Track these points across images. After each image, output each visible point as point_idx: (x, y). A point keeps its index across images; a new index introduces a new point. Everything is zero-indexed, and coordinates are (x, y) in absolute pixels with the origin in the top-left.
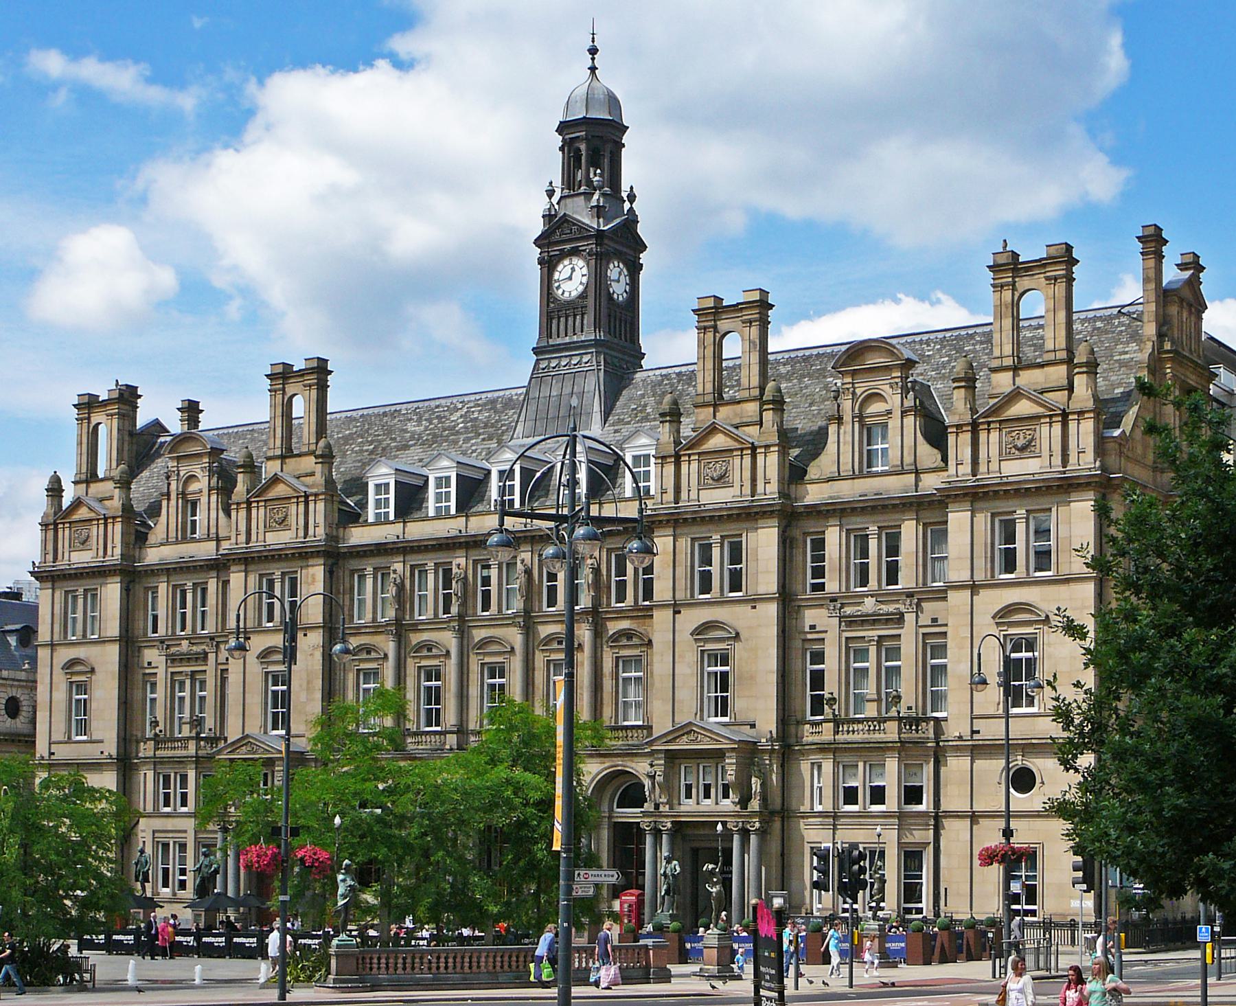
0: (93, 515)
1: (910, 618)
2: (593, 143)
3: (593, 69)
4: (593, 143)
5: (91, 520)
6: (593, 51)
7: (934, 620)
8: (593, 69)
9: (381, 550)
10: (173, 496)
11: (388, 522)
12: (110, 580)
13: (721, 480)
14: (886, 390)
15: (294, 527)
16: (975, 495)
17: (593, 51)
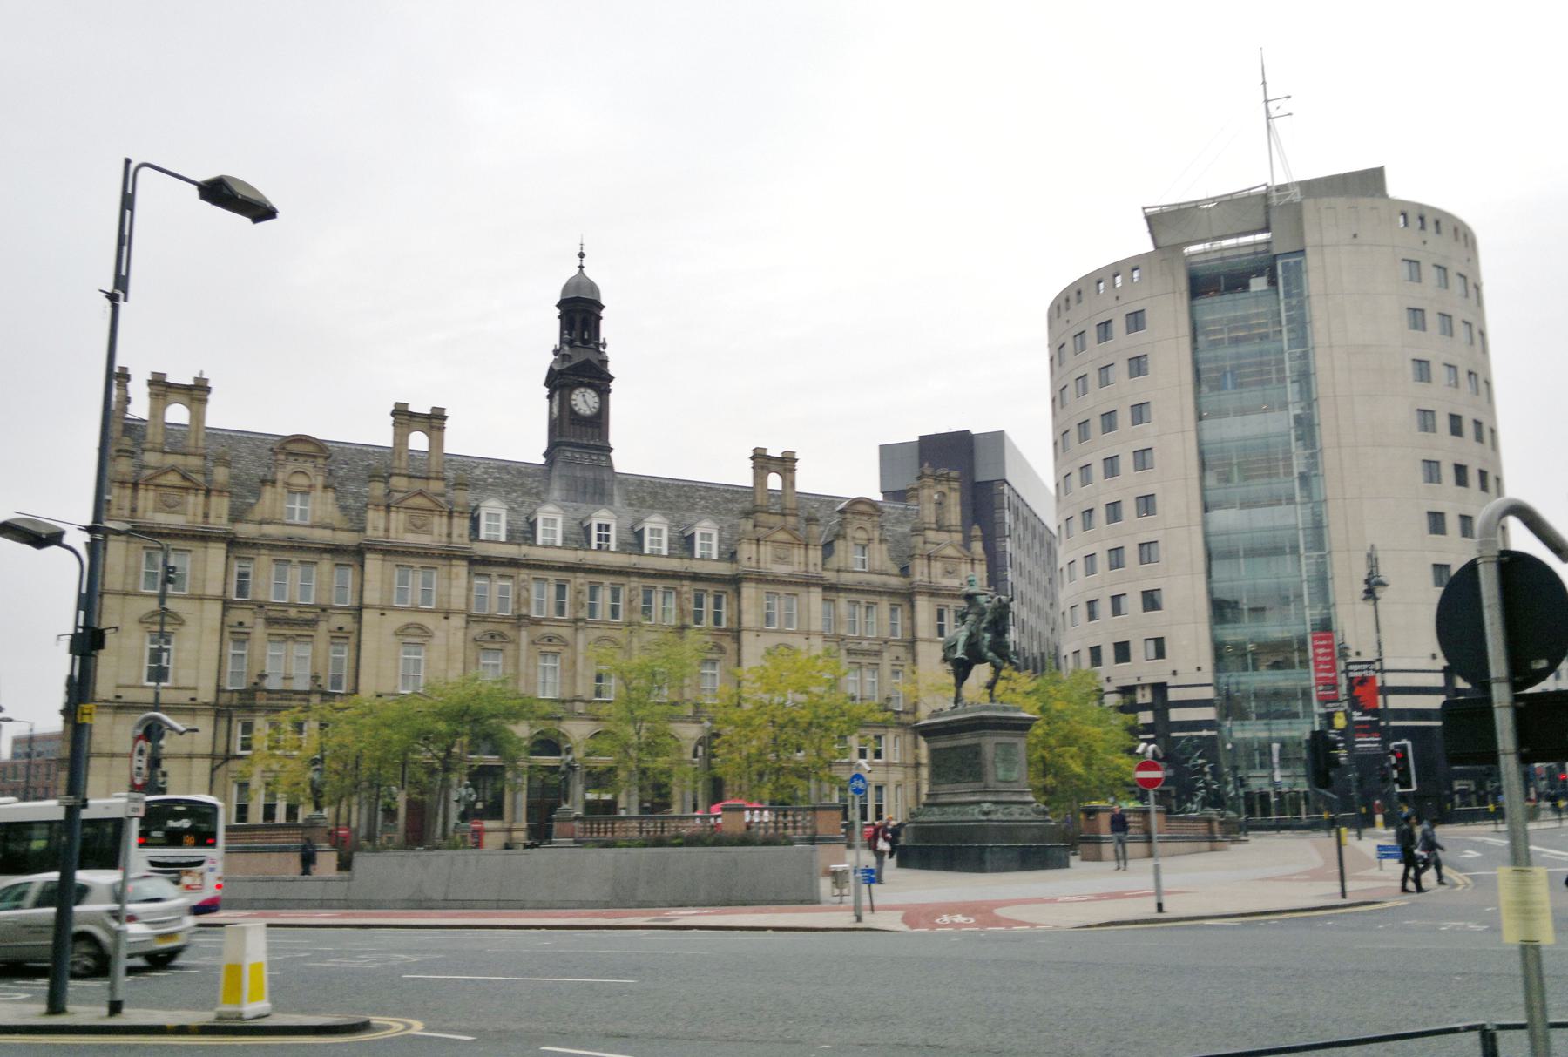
0: (187, 484)
1: (886, 655)
2: (580, 313)
3: (581, 267)
4: (580, 313)
5: (187, 489)
6: (581, 255)
8: (581, 267)
9: (513, 563)
10: (279, 484)
11: (553, 546)
12: (211, 545)
13: (781, 560)
14: (868, 525)
15: (436, 530)
16: (934, 592)
17: (581, 255)
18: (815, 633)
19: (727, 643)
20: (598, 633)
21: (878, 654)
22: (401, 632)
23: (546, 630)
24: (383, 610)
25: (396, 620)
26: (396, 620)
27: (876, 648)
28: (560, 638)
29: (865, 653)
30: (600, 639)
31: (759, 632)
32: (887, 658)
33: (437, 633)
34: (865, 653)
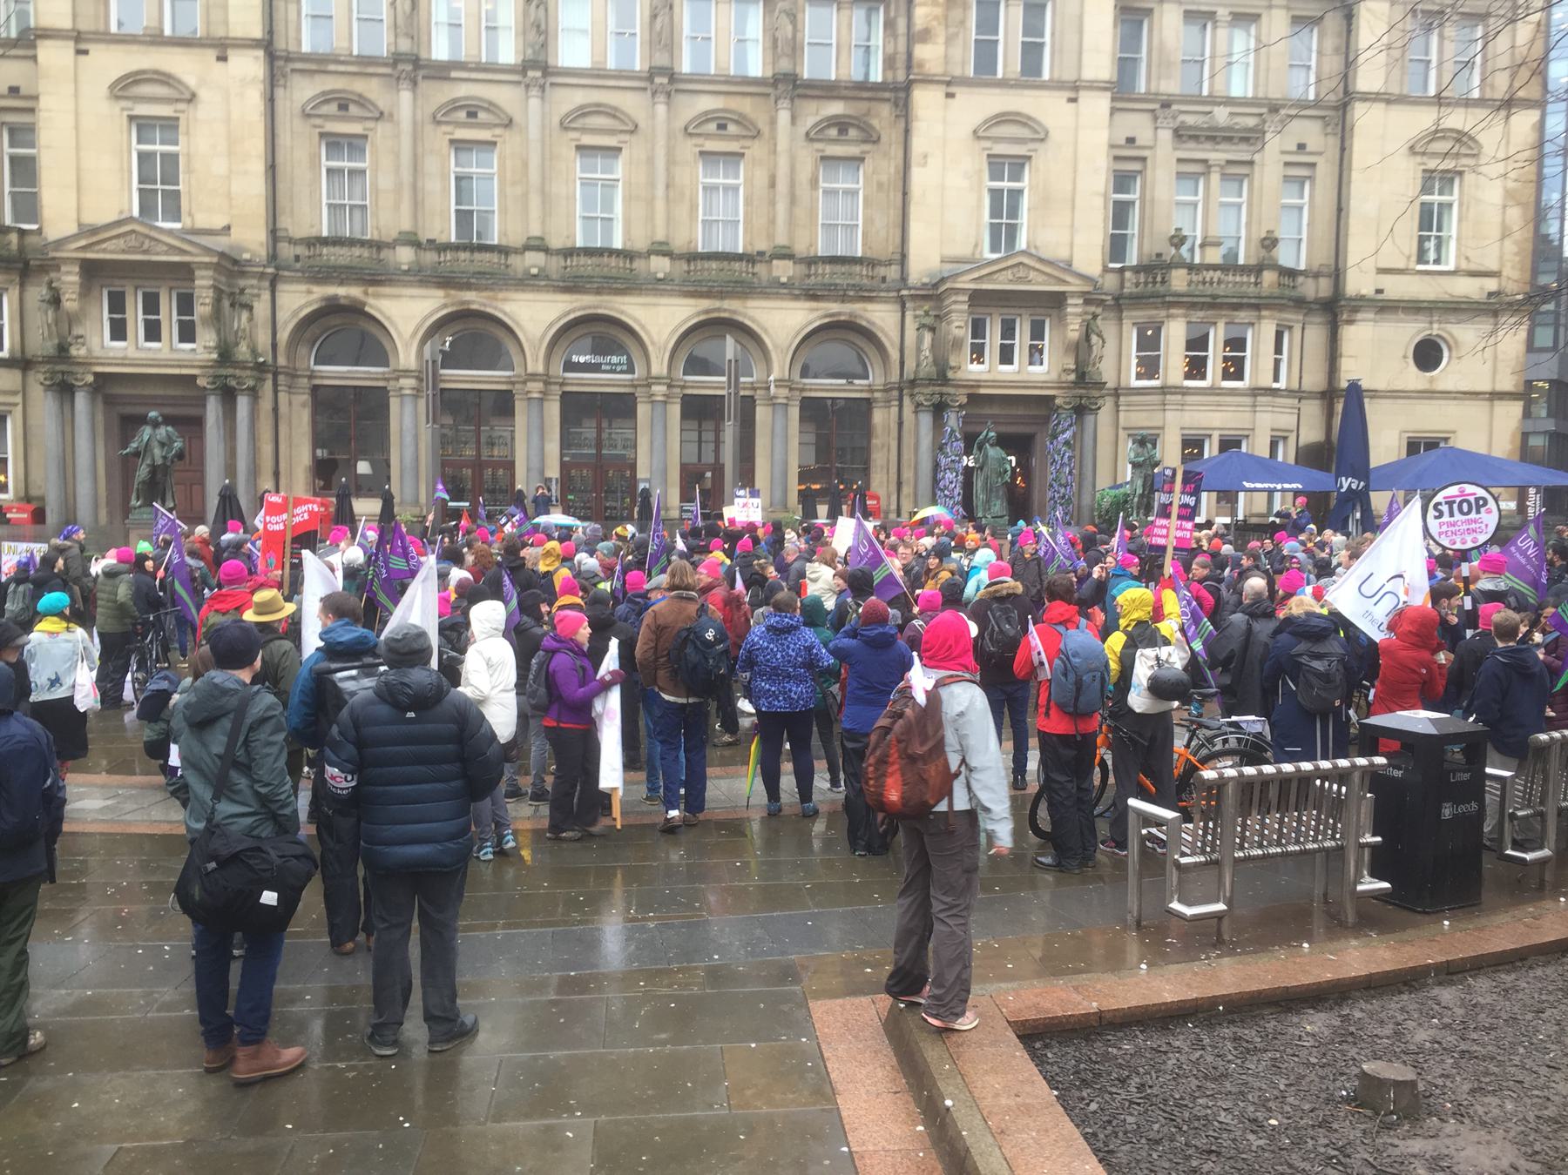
7: (1301, 147)
18: (1093, 86)
19: (882, 117)
20: (579, 98)
21: (1252, 138)
22: (124, 87)
23: (463, 90)
24: (80, 40)
25: (110, 63)
26: (110, 63)
27: (1251, 122)
28: (491, 107)
29: (1216, 136)
30: (583, 112)
31: (950, 84)
32: (1275, 148)
33: (203, 94)
34: (1216, 136)
